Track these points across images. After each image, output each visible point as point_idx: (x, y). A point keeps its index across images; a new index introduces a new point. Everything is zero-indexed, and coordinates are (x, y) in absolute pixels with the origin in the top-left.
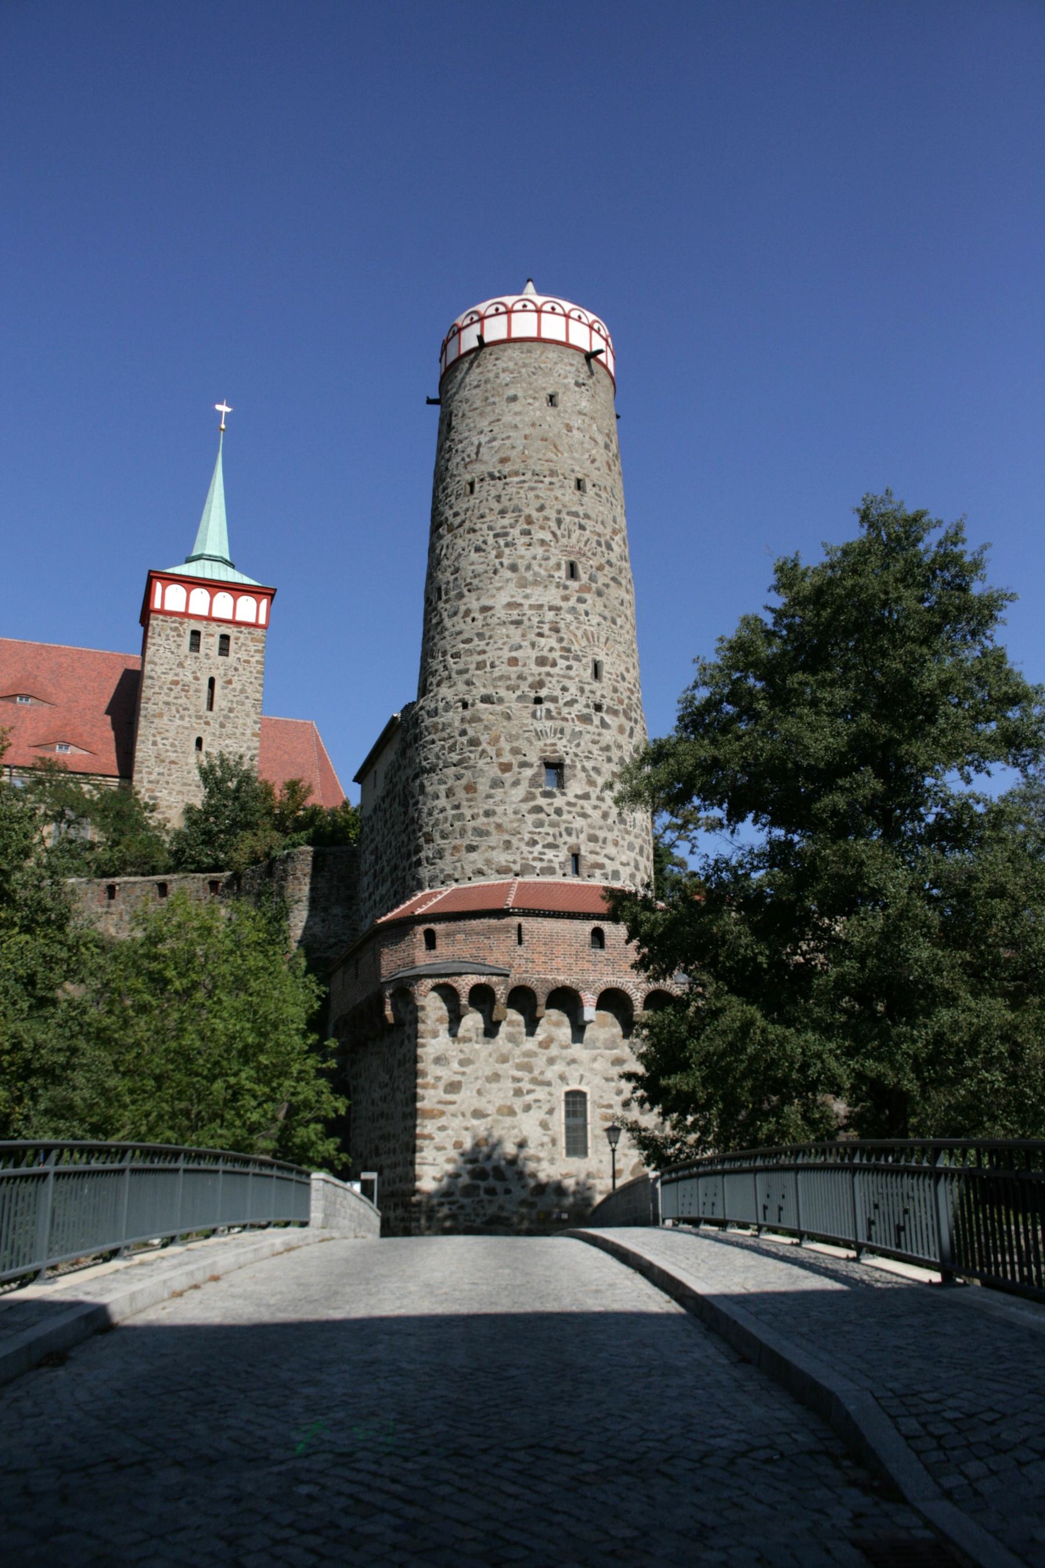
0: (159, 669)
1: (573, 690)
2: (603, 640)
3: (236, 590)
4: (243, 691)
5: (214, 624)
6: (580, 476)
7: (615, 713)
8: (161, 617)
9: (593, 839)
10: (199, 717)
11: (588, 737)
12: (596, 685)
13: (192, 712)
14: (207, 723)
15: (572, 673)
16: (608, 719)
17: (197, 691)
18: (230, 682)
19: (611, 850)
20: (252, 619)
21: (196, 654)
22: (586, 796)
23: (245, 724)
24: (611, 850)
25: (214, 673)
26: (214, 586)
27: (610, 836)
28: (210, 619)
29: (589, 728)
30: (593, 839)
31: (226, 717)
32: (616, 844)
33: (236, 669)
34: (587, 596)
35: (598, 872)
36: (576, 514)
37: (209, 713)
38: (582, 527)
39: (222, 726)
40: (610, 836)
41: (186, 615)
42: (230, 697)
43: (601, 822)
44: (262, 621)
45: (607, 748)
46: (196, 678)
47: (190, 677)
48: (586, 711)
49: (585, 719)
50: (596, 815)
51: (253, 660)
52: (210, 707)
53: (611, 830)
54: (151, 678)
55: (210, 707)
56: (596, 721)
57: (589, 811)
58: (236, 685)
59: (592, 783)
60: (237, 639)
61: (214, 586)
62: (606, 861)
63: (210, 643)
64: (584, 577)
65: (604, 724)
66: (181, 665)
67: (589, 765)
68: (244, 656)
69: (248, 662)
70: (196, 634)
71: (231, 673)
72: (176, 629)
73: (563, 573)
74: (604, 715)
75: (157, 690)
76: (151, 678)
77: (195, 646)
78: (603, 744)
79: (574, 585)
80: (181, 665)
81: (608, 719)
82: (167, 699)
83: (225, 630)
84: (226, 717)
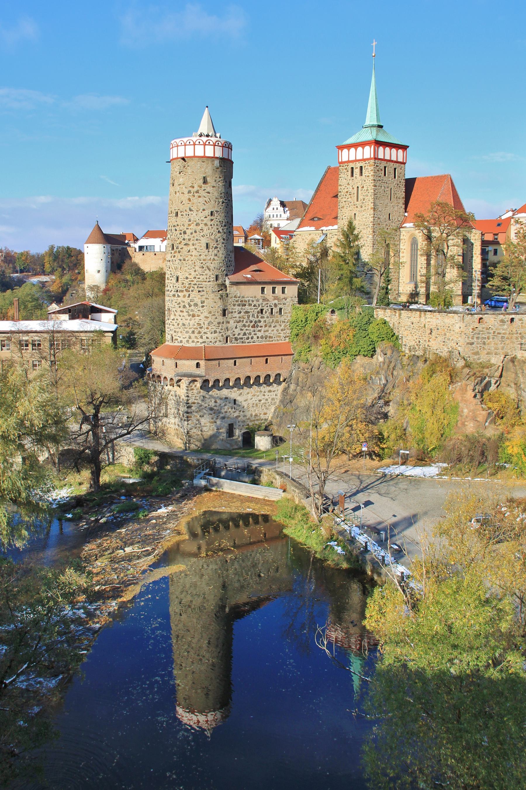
0: (343, 187)
1: (172, 287)
2: (179, 268)
3: (363, 144)
4: (367, 190)
5: (357, 163)
6: (176, 211)
7: (182, 291)
8: (342, 165)
9: (175, 332)
10: (354, 205)
11: (174, 301)
12: (177, 284)
13: (352, 203)
14: (357, 207)
15: (172, 281)
16: (179, 294)
17: (354, 194)
18: (363, 187)
19: (180, 334)
20: (369, 157)
21: (352, 178)
22: (173, 320)
23: (368, 205)
24: (180, 334)
25: (359, 185)
26: (356, 146)
27: (179, 330)
28: (356, 161)
29: (175, 298)
30: (175, 332)
31: (363, 203)
32: (181, 332)
33: (365, 181)
34: (176, 254)
35: (176, 341)
36: (174, 226)
37: (357, 203)
38: (176, 230)
39: (361, 207)
40: (179, 330)
41: (349, 162)
42: (364, 194)
43: (177, 327)
44: (372, 156)
45: (179, 303)
46: (353, 188)
47: (351, 188)
48: (174, 293)
49: (174, 295)
50: (176, 324)
51: (370, 175)
52: (357, 201)
53: (180, 328)
54: (340, 192)
55: (357, 201)
56: (176, 296)
57: (175, 324)
58: (365, 188)
59: (175, 315)
60: (365, 167)
61: (356, 146)
62: (178, 338)
63: (357, 171)
64: (175, 248)
65: (178, 296)
66: (348, 184)
67: (174, 310)
68: (367, 175)
69: (368, 176)
70: (352, 168)
71: (364, 182)
72: (346, 169)
73: (171, 249)
74: (178, 293)
75: (342, 197)
76: (340, 192)
77: (352, 176)
78: (178, 303)
79: (173, 252)
80: (348, 184)
81: (179, 294)
82: (345, 200)
83: (362, 164)
84: (363, 203)
